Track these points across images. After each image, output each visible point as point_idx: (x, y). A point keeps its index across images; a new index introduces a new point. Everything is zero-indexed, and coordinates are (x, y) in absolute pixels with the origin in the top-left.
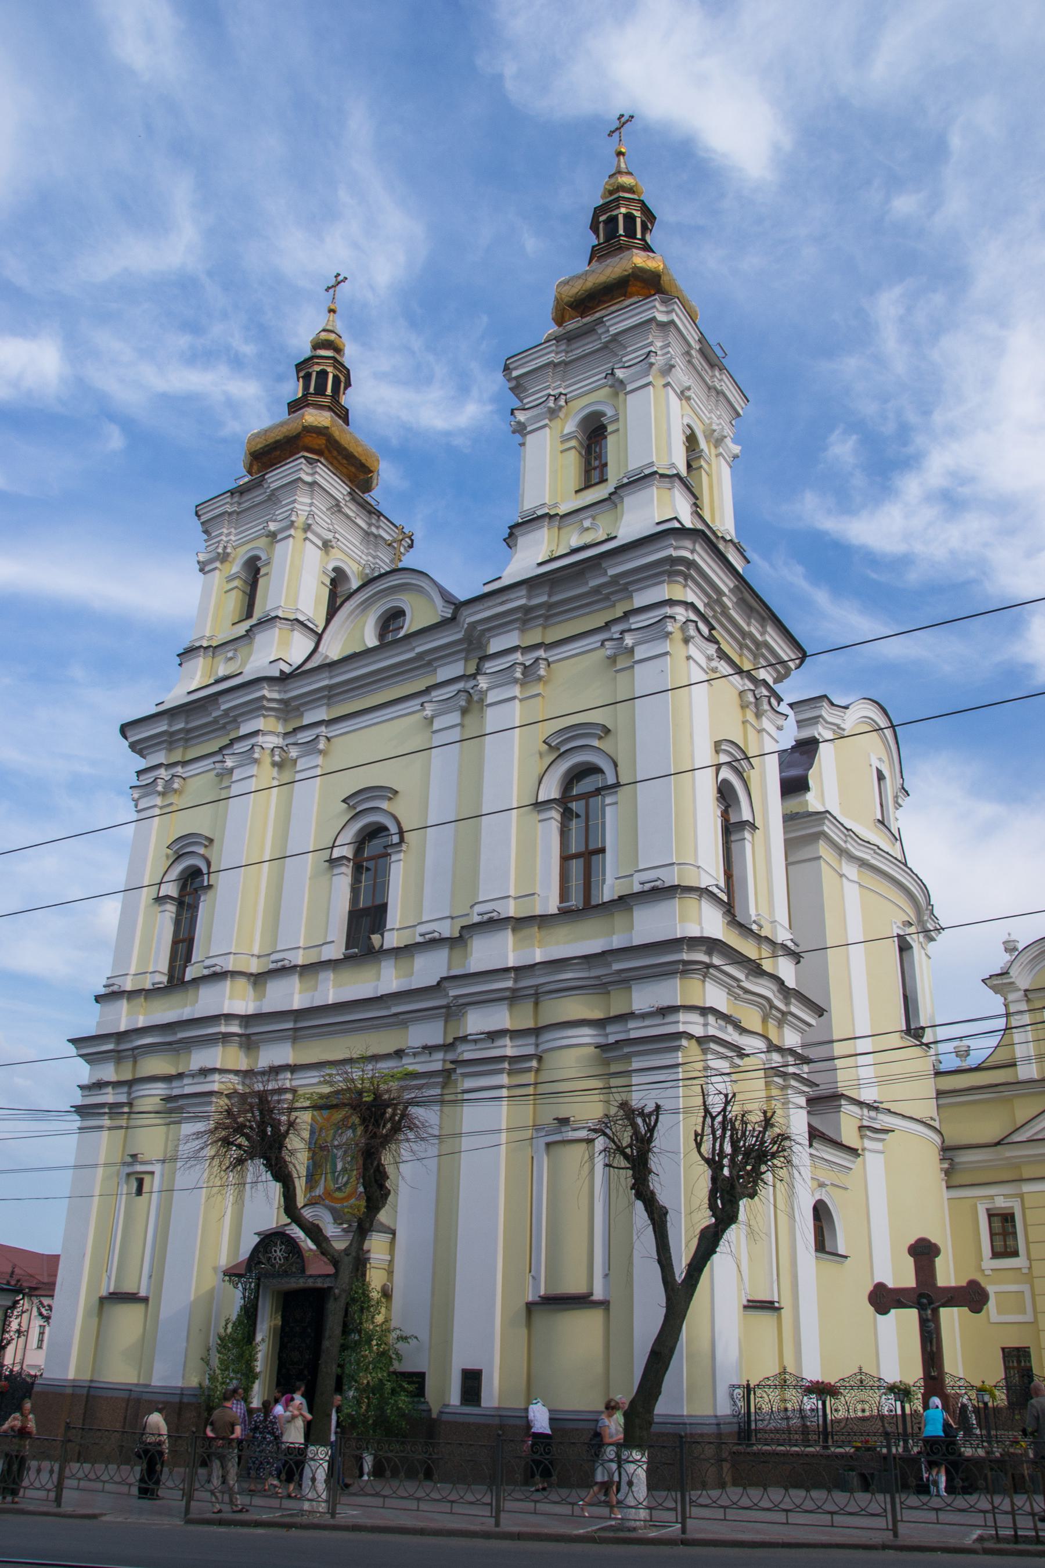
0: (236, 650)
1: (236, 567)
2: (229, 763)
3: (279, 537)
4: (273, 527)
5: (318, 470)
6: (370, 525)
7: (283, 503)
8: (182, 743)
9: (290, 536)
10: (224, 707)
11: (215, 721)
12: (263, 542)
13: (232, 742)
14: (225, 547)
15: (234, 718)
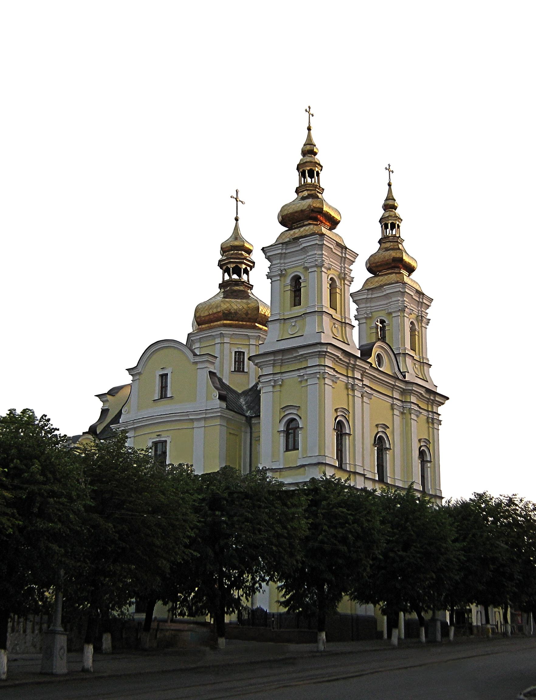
0: (296, 322)
1: (288, 281)
2: (305, 378)
3: (310, 270)
4: (306, 265)
5: (325, 238)
6: (342, 253)
7: (310, 254)
8: (280, 364)
9: (315, 271)
10: (300, 353)
11: (296, 357)
12: (300, 269)
13: (305, 368)
14: (281, 271)
15: (305, 357)
